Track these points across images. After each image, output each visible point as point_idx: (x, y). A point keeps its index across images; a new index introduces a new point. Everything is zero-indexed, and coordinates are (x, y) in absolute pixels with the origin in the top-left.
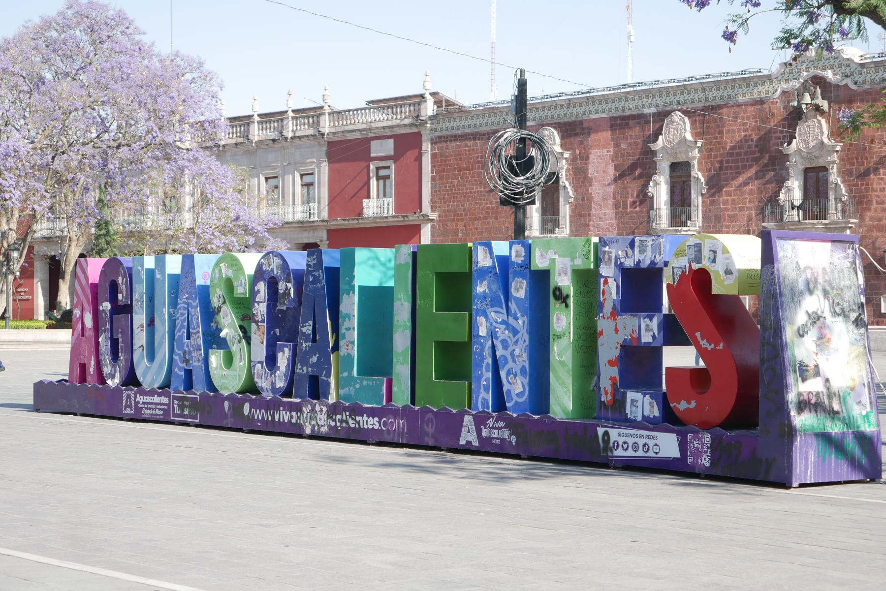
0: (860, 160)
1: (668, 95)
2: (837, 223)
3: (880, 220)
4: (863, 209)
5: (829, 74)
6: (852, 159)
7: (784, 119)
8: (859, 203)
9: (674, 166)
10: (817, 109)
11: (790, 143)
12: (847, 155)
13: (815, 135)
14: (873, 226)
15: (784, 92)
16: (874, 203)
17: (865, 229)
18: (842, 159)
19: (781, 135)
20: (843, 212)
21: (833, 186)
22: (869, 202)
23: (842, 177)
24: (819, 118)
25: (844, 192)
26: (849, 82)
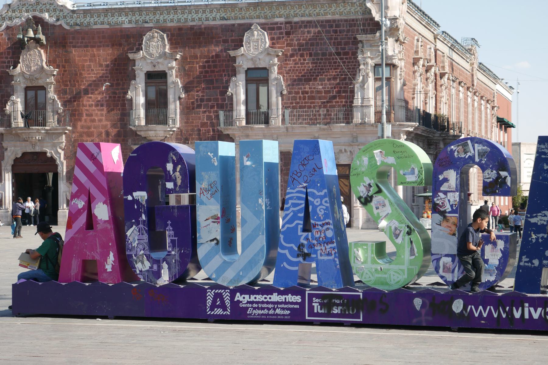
0: (72, 83)
1: (197, 12)
2: (56, 130)
3: (89, 128)
4: (75, 120)
5: (46, 16)
6: (66, 81)
7: (9, 48)
8: (72, 115)
9: (149, 76)
10: (37, 41)
11: (15, 67)
12: (62, 79)
13: (35, 62)
14: (84, 132)
15: (8, 28)
16: (85, 115)
17: (78, 134)
18: (57, 81)
19: (7, 60)
20: (59, 122)
21: (51, 101)
22: (81, 115)
23: (58, 95)
24: (39, 49)
25: (60, 106)
26: (62, 22)
